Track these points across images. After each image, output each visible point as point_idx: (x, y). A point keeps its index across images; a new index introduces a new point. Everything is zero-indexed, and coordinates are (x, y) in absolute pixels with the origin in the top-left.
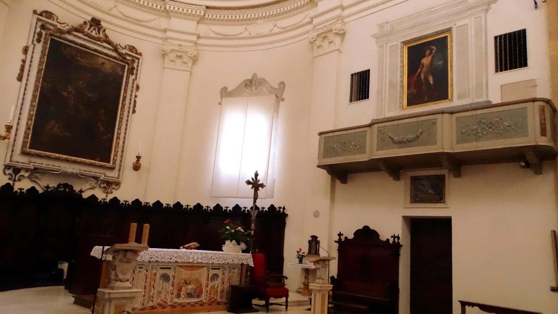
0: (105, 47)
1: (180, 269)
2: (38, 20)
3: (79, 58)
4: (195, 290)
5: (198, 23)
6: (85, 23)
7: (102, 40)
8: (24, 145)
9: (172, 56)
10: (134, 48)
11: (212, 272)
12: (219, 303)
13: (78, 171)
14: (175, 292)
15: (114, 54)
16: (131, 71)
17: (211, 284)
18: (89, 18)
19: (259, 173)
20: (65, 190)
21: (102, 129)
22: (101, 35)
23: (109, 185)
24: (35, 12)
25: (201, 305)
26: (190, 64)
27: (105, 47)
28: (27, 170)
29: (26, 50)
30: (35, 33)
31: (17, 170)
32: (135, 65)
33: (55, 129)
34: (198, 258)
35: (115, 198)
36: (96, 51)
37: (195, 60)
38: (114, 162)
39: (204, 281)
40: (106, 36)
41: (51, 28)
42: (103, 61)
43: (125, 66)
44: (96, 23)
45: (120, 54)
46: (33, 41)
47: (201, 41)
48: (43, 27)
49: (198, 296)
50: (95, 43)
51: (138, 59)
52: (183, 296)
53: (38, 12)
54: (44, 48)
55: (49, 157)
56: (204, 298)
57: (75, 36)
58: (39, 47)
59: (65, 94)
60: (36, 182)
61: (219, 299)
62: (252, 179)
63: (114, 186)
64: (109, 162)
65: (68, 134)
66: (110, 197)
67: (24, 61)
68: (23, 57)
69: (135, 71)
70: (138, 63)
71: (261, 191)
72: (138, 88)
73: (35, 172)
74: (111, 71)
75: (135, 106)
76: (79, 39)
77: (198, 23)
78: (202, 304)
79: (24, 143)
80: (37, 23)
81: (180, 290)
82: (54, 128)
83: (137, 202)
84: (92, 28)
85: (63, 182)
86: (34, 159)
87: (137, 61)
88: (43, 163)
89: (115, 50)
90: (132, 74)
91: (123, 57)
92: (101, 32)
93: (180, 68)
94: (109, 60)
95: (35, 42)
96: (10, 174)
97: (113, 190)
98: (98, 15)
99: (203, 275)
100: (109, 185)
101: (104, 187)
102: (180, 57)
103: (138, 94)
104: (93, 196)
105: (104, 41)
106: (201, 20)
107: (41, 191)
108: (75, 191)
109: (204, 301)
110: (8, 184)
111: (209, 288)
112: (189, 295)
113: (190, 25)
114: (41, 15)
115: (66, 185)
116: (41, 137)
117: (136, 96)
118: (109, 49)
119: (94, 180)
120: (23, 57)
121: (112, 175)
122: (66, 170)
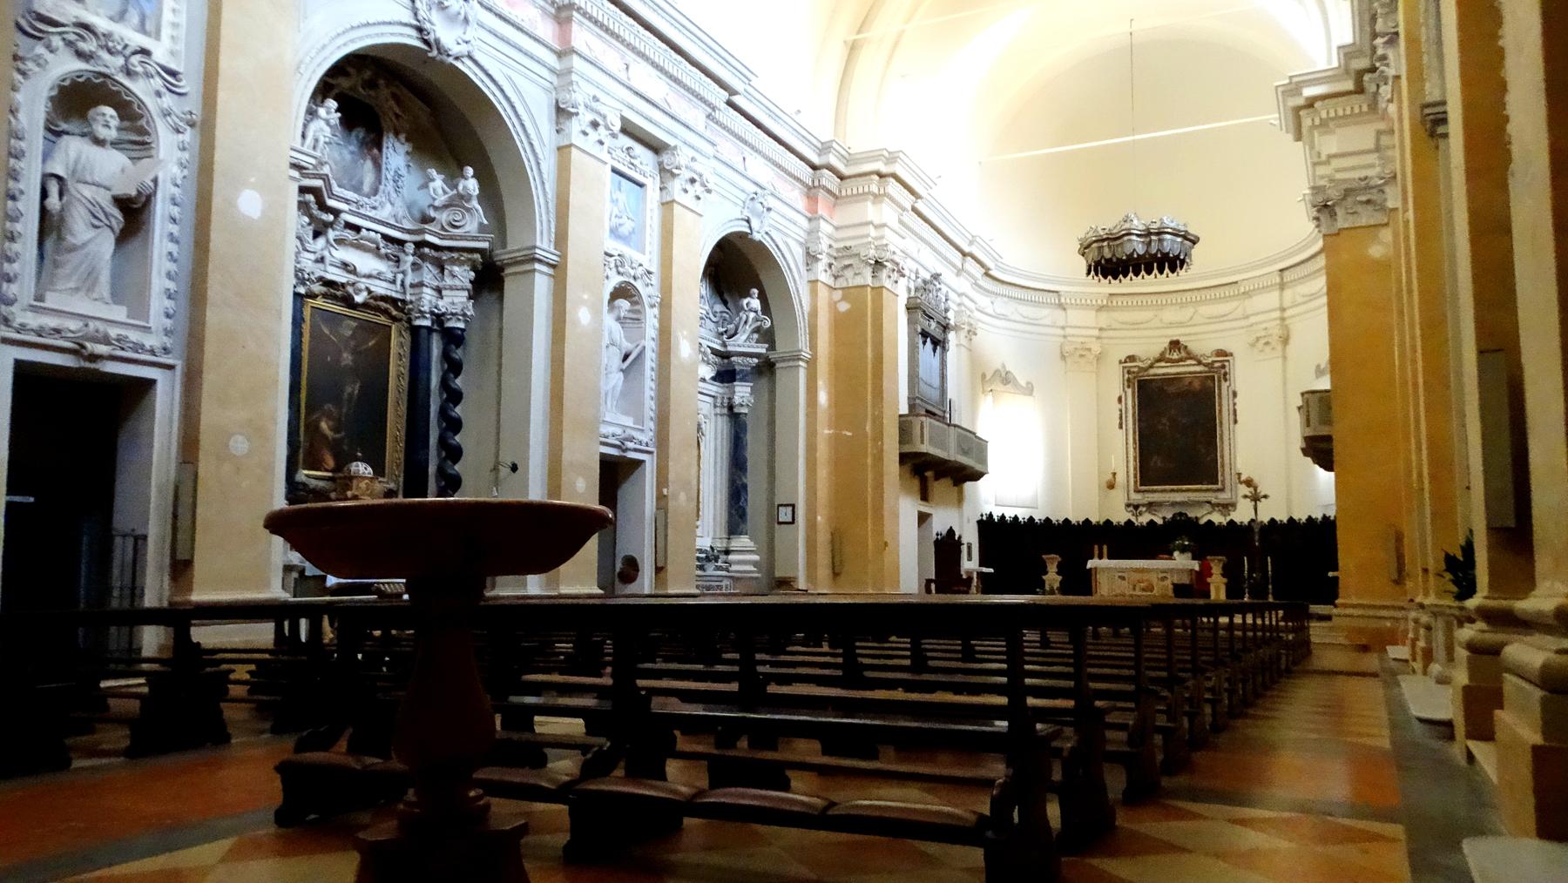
9: (1260, 344)
15: (1198, 368)
22: (1183, 354)
23: (1227, 507)
26: (1279, 348)
29: (1120, 400)
31: (1136, 507)
35: (1232, 522)
37: (1285, 340)
39: (1155, 581)
40: (1188, 353)
44: (1175, 344)
47: (1288, 313)
58: (1129, 391)
71: (1261, 505)
72: (1235, 395)
73: (1151, 506)
76: (1163, 370)
82: (1157, 461)
85: (1177, 510)
89: (1200, 363)
98: (1175, 334)
99: (1154, 578)
100: (1227, 507)
102: (1267, 343)
106: (1282, 286)
107: (1160, 522)
110: (1129, 522)
113: (1272, 299)
115: (1181, 514)
116: (1148, 474)
121: (1224, 497)
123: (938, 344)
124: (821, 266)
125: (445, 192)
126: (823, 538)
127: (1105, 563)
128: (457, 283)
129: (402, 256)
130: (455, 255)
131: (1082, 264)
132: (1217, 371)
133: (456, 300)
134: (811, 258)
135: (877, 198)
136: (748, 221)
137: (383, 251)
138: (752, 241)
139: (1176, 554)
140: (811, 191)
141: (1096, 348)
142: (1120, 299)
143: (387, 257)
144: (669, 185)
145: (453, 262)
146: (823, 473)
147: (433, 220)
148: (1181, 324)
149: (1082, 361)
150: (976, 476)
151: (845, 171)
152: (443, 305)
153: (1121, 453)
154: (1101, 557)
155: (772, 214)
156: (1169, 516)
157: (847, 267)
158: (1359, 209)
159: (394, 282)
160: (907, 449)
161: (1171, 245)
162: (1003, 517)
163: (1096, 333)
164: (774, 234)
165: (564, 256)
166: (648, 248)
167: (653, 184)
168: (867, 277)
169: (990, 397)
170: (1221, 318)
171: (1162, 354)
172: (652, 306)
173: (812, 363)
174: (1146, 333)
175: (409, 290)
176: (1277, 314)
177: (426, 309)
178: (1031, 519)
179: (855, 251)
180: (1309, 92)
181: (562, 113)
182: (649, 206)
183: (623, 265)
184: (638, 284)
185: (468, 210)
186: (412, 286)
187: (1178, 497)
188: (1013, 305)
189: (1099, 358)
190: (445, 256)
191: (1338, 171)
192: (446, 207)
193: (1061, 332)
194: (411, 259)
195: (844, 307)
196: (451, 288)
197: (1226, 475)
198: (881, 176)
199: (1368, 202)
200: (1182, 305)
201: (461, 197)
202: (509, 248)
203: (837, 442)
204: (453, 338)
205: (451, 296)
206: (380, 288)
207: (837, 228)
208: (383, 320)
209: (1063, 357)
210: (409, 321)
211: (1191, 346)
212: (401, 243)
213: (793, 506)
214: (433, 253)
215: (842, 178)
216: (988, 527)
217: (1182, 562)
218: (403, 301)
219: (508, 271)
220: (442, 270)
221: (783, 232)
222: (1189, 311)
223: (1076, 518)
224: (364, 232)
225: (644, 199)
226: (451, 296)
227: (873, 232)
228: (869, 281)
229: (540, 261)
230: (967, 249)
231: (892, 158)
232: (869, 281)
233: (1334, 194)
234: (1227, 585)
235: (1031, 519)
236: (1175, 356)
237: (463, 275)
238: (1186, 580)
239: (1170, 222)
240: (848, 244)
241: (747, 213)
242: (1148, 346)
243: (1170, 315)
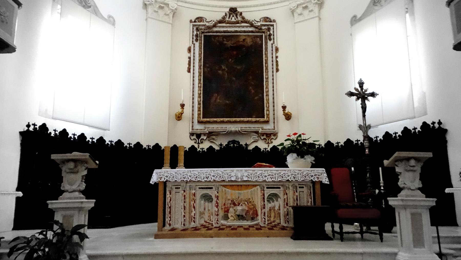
0: (243, 27)
1: (224, 189)
2: (194, 26)
3: (225, 42)
4: (248, 212)
6: (226, 15)
7: (240, 22)
8: (199, 117)
9: (299, 10)
10: (268, 18)
11: (268, 192)
12: (283, 228)
13: (240, 129)
14: (221, 213)
17: (269, 206)
18: (228, 10)
19: (364, 80)
20: (234, 145)
21: (253, 91)
22: (240, 19)
23: (269, 136)
24: (191, 21)
25: (257, 229)
27: (243, 27)
28: (205, 134)
29: (189, 50)
30: (193, 35)
31: (198, 136)
32: (271, 32)
33: (218, 100)
34: (243, 176)
36: (236, 32)
38: (268, 117)
39: (259, 204)
40: (243, 18)
41: (203, 28)
42: (244, 38)
43: (262, 36)
44: (233, 11)
45: (256, 27)
46: (193, 42)
48: (197, 30)
49: (253, 219)
50: (235, 27)
51: (273, 25)
52: (231, 218)
53: (193, 21)
54: (200, 44)
55: (216, 122)
56: (260, 220)
57: (220, 27)
58: (197, 44)
59: (220, 72)
60: (212, 142)
61: (283, 223)
62: (356, 89)
63: (272, 137)
64: (264, 118)
65: (227, 102)
66: (271, 146)
67: (190, 58)
68: (189, 55)
69: (272, 37)
70: (273, 29)
72: (277, 50)
73: (210, 135)
74: (252, 43)
75: (277, 65)
78: (259, 228)
79: (199, 114)
80: (193, 29)
81: (227, 211)
84: (231, 16)
86: (208, 126)
87: (272, 28)
89: (252, 25)
90: (270, 40)
91: (259, 29)
92: (238, 17)
93: (309, 18)
94: (248, 35)
95: (195, 42)
96: (194, 139)
97: (273, 140)
98: (233, 4)
99: (256, 196)
100: (269, 136)
101: (264, 139)
103: (278, 55)
104: (257, 148)
105: (242, 22)
107: (217, 148)
108: (242, 145)
109: (262, 225)
110: (193, 146)
111: (266, 210)
112: (240, 217)
114: (195, 22)
115: (234, 142)
117: (277, 57)
118: (247, 27)
119: (256, 135)
120: (189, 55)
121: (268, 127)
122: (230, 129)
132: (264, 31)
149: (161, 12)
153: (187, 87)
154: (174, 165)
156: (225, 143)
171: (224, 18)
189: (174, 13)
211: (243, 14)
234: (432, 211)
235: (101, 140)
236: (233, 19)
238: (306, 200)
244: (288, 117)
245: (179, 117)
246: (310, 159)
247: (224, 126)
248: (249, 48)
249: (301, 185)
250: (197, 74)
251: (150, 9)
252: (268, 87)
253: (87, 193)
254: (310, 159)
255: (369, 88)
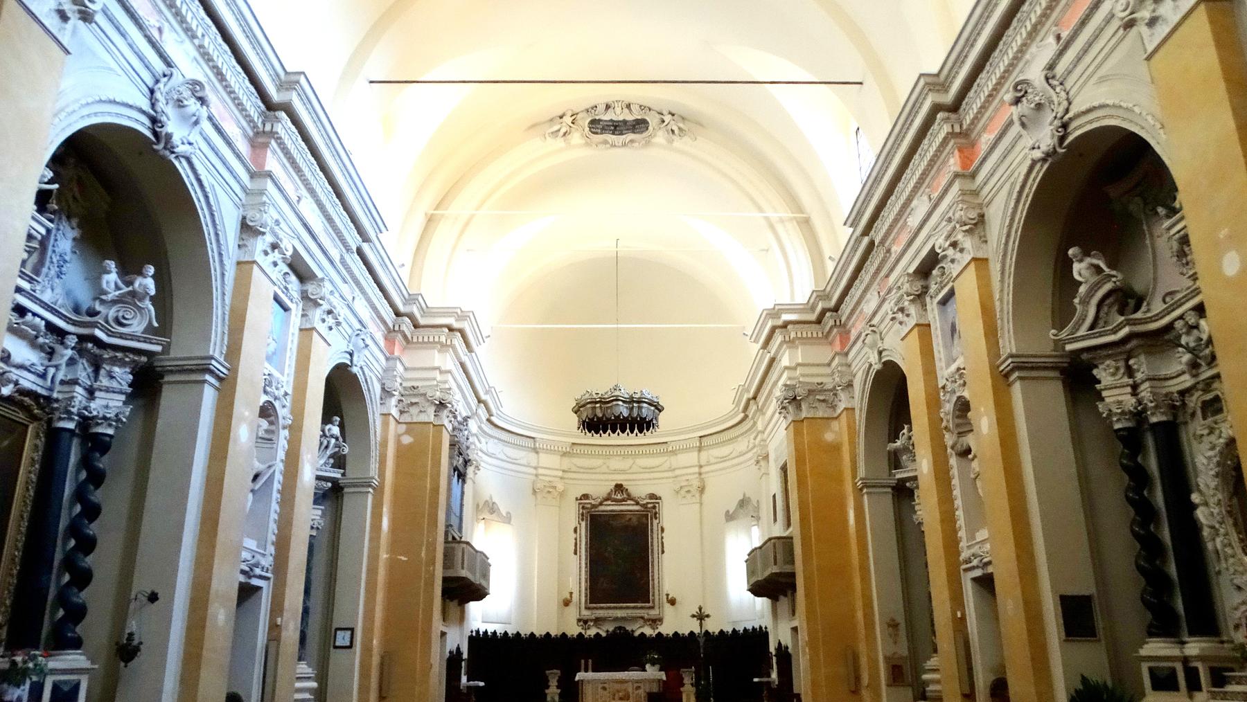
5: (700, 451)
9: (683, 492)
16: (656, 515)
23: (655, 622)
26: (697, 495)
31: (586, 622)
37: (702, 490)
39: (630, 690)
40: (629, 495)
44: (619, 487)
45: (642, 505)
47: (703, 470)
55: (602, 608)
58: (583, 524)
72: (663, 530)
73: (598, 621)
76: (610, 507)
77: (700, 451)
83: (676, 634)
85: (618, 624)
88: (601, 613)
98: (619, 478)
104: (642, 634)
106: (700, 449)
107: (604, 634)
110: (580, 634)
113: (692, 458)
115: (620, 628)
123: (462, 476)
124: (394, 401)
125: (117, 288)
126: (376, 660)
127: (590, 675)
128: (114, 384)
129: (58, 347)
130: (119, 355)
131: (574, 420)
133: (111, 404)
134: (387, 394)
135: (444, 347)
136: (351, 355)
137: (41, 340)
138: (350, 372)
139: (648, 666)
140: (390, 333)
141: (560, 487)
142: (579, 448)
143: (41, 348)
144: (310, 313)
145: (114, 361)
146: (380, 596)
147: (97, 313)
148: (623, 472)
150: (479, 593)
151: (422, 321)
152: (96, 407)
154: (586, 671)
155: (366, 352)
156: (611, 629)
157: (412, 404)
158: (817, 404)
159: (43, 376)
160: (451, 573)
161: (646, 411)
162: (486, 632)
163: (560, 474)
164: (366, 369)
165: (234, 370)
166: (286, 371)
167: (296, 309)
168: (429, 416)
169: (481, 525)
170: (650, 469)
172: (284, 428)
173: (379, 491)
174: (593, 476)
175: (58, 387)
176: (696, 470)
177: (74, 410)
178: (506, 633)
179: (422, 391)
180: (786, 317)
181: (248, 229)
182: (291, 330)
183: (270, 384)
184: (277, 404)
185: (140, 309)
186: (63, 382)
187: (619, 613)
188: (500, 446)
189: (562, 495)
190: (107, 355)
191: (803, 375)
192: (114, 302)
193: (534, 472)
194: (69, 352)
195: (407, 440)
196: (108, 390)
197: (655, 594)
198: (451, 329)
199: (824, 401)
200: (624, 456)
201: (133, 294)
202: (172, 355)
203: (393, 565)
204: (95, 444)
205: (110, 401)
206: (28, 381)
207: (406, 369)
208: (21, 416)
209: (534, 492)
210: (50, 421)
212: (60, 334)
213: (352, 630)
214: (96, 351)
215: (416, 326)
216: (480, 641)
217: (653, 673)
218: (48, 399)
219: (167, 378)
220: (97, 371)
221: (370, 368)
222: (630, 461)
223: (539, 632)
224: (29, 317)
225: (286, 323)
226: (110, 401)
227: (439, 377)
228: (432, 418)
229: (211, 372)
230: (483, 397)
231: (462, 316)
232: (432, 418)
233: (801, 391)
235: (506, 633)
236: (619, 497)
237: (123, 376)
238: (655, 689)
239: (649, 393)
240: (415, 384)
241: (351, 347)
242: (599, 488)
243: (616, 464)
244: (672, 602)
245: (567, 603)
246: (657, 667)
247: (611, 612)
248: (634, 528)
249: (653, 681)
250: (583, 557)
251: (539, 496)
252: (654, 572)
253: (558, 687)
254: (657, 667)
255: (706, 611)
